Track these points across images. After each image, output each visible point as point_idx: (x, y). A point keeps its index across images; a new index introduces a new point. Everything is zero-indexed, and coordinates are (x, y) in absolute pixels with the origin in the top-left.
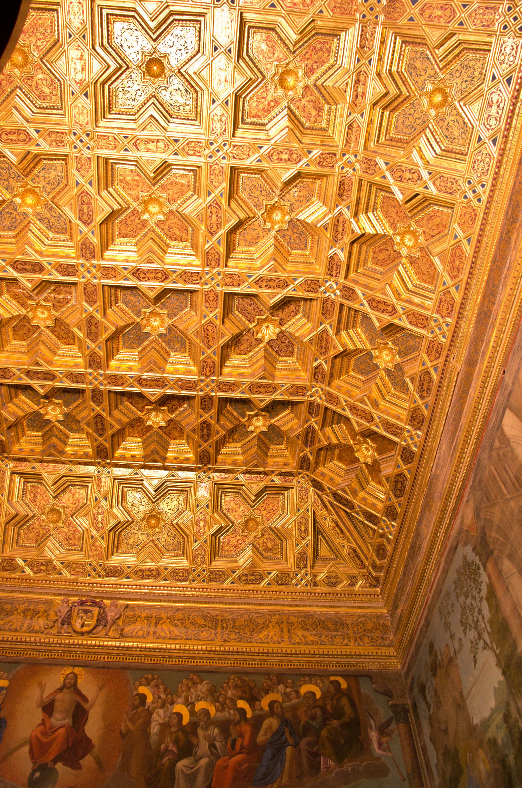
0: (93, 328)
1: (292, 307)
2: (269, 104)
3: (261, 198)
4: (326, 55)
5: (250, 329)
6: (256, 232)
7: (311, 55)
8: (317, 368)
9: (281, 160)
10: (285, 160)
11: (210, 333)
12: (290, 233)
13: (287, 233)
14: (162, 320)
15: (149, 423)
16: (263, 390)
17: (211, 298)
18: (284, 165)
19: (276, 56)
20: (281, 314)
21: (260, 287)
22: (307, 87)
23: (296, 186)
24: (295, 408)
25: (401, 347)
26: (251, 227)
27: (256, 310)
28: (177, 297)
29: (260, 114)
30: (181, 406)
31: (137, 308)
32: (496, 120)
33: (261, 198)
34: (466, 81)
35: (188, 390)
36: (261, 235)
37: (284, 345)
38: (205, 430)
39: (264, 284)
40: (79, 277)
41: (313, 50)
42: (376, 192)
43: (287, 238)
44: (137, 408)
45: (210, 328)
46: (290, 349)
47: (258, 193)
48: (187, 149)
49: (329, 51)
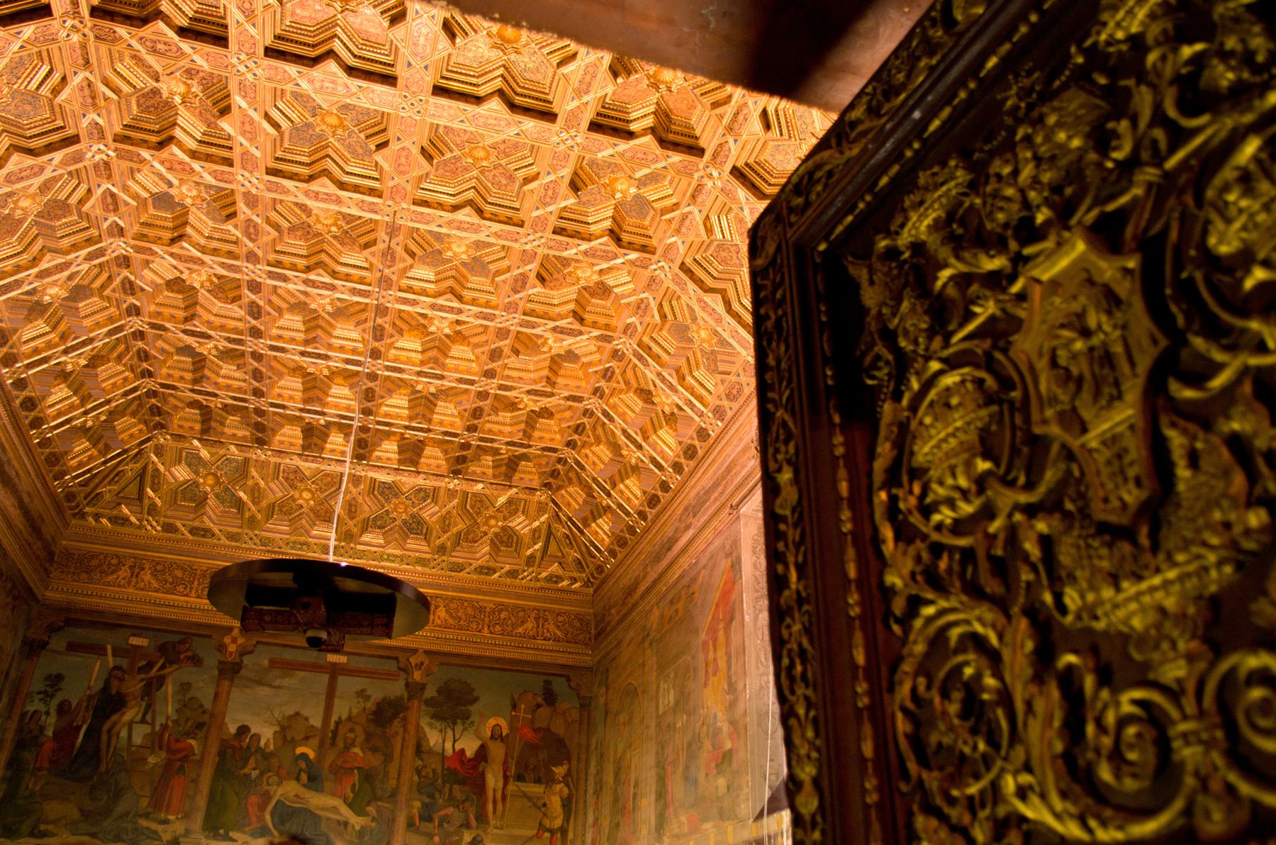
49: (139, 105)
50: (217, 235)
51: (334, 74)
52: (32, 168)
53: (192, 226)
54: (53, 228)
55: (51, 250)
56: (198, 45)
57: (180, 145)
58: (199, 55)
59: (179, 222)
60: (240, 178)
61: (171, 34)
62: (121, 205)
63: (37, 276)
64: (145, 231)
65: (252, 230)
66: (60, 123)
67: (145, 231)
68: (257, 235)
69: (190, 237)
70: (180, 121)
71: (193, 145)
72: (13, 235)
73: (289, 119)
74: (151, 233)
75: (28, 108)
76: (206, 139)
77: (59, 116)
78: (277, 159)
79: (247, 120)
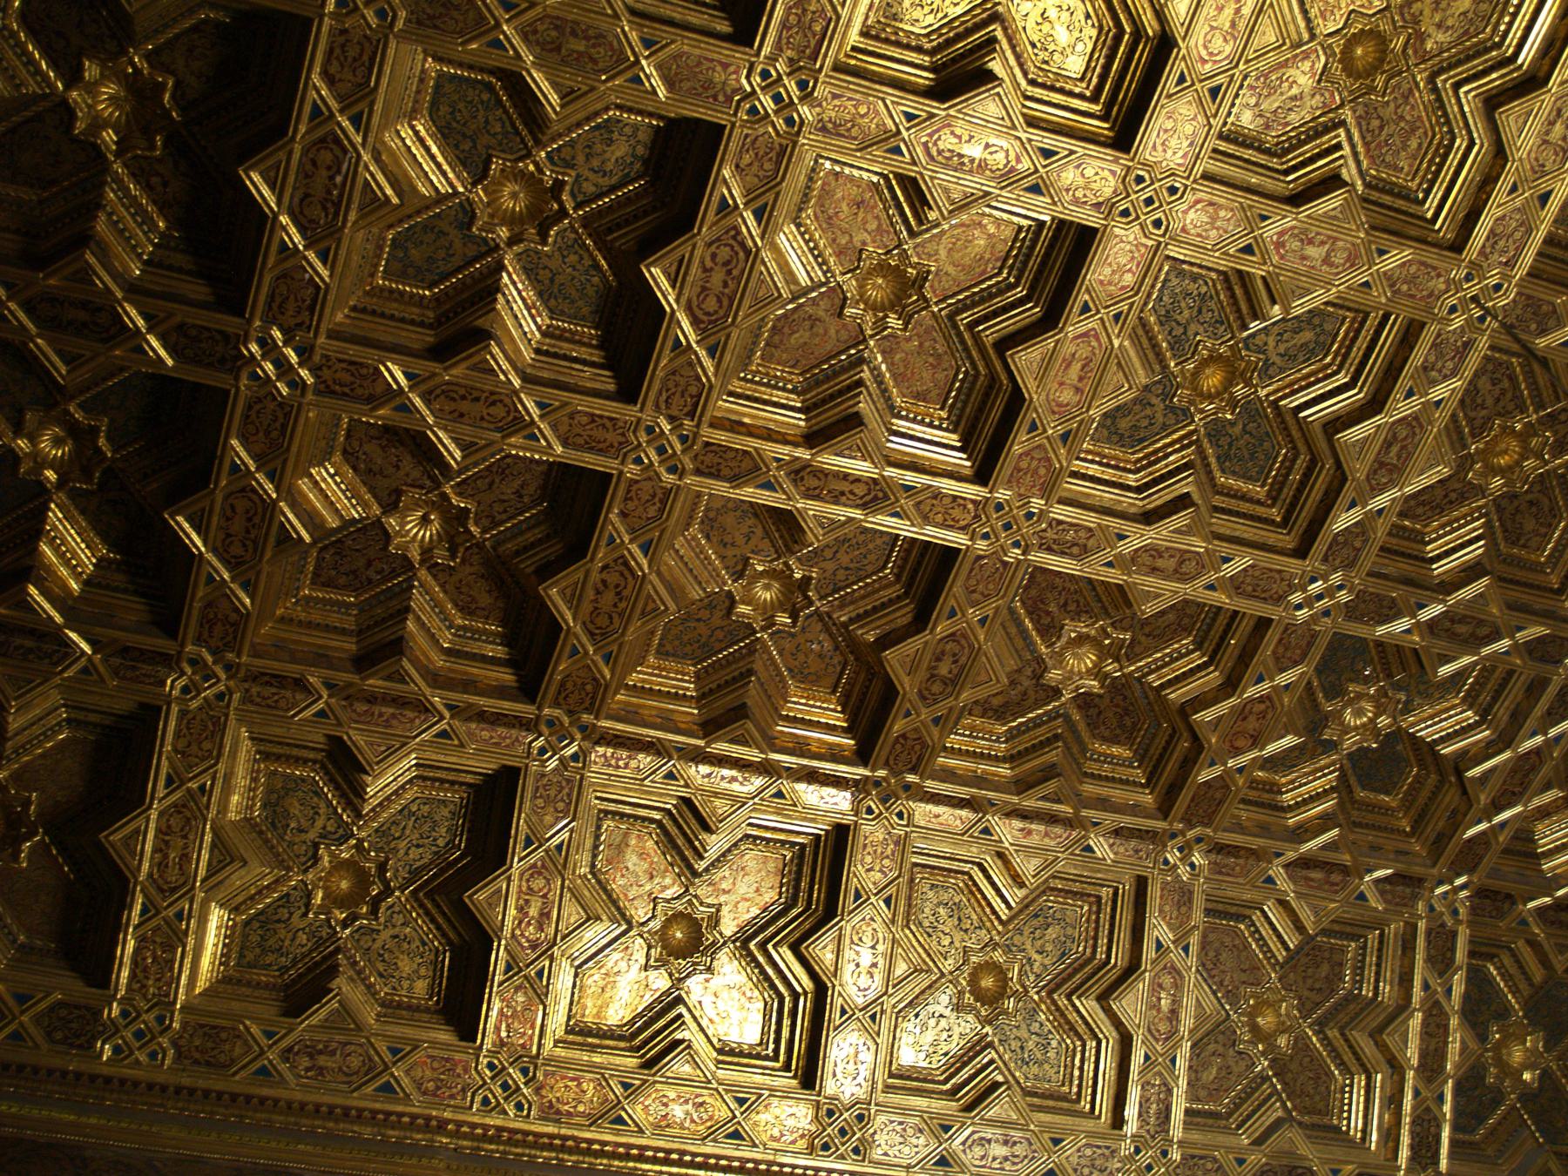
0: (580, 46)
1: (485, 600)
2: (1048, 613)
3: (830, 566)
4: (1107, 734)
5: (438, 485)
6: (740, 540)
7: (1117, 706)
8: (300, 685)
9: (938, 659)
10: (935, 668)
11: (480, 409)
12: (717, 621)
13: (718, 614)
14: (511, 220)
15: (91, 70)
16: (238, 526)
17: (599, 434)
18: (925, 665)
19: (1143, 639)
20: (468, 569)
21: (605, 567)
22: (1056, 692)
23: (837, 648)
24: (119, 579)
25: (386, 935)
26: (759, 531)
27: (497, 507)
28: (591, 291)
29: (1033, 592)
30: (163, 209)
31: (581, 159)
32: (983, 1157)
33: (830, 566)
34: (1022, 1048)
35: (271, 297)
36: (730, 552)
37: (361, 563)
38: (83, 316)
39: (613, 578)
40: (772, 59)
41: (1126, 709)
42: (793, 844)
43: (705, 614)
44: (170, 44)
45: (499, 411)
46: (342, 580)
47: (845, 559)
48: (1037, 455)
50: (1485, 698)
51: (1048, 361)
52: (1156, 987)
53: (1442, 740)
54: (1350, 998)
55: (1381, 1029)
56: (947, 601)
57: (1202, 701)
58: (964, 613)
59: (1429, 760)
60: (1303, 614)
61: (914, 644)
62: (1332, 856)
63: (1429, 1081)
64: (1431, 831)
65: (1462, 629)
66: (1105, 893)
67: (1431, 831)
68: (1481, 623)
69: (1463, 753)
70: (1154, 680)
71: (1213, 677)
72: (1330, 1074)
73: (1178, 470)
74: (1437, 824)
75: (1052, 933)
76: (1209, 646)
77: (1090, 890)
78: (1285, 522)
79: (1146, 558)
